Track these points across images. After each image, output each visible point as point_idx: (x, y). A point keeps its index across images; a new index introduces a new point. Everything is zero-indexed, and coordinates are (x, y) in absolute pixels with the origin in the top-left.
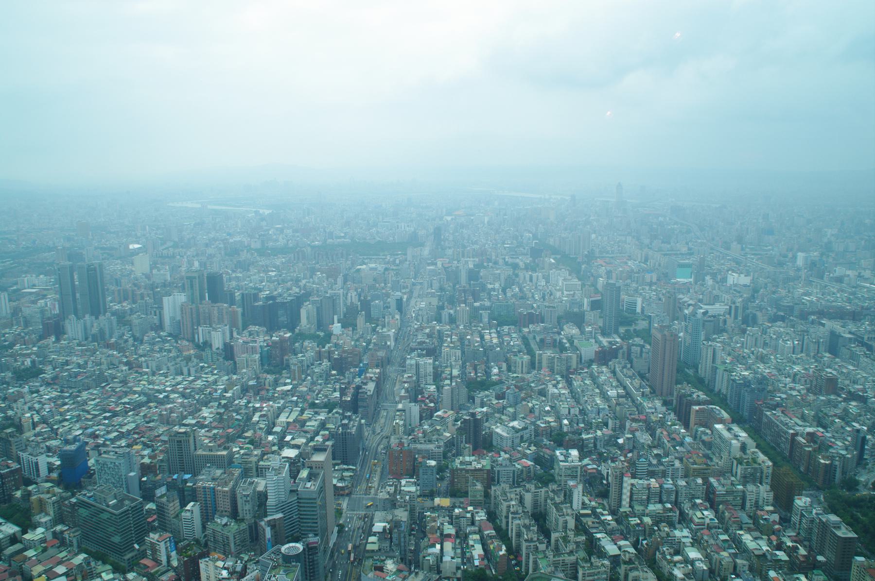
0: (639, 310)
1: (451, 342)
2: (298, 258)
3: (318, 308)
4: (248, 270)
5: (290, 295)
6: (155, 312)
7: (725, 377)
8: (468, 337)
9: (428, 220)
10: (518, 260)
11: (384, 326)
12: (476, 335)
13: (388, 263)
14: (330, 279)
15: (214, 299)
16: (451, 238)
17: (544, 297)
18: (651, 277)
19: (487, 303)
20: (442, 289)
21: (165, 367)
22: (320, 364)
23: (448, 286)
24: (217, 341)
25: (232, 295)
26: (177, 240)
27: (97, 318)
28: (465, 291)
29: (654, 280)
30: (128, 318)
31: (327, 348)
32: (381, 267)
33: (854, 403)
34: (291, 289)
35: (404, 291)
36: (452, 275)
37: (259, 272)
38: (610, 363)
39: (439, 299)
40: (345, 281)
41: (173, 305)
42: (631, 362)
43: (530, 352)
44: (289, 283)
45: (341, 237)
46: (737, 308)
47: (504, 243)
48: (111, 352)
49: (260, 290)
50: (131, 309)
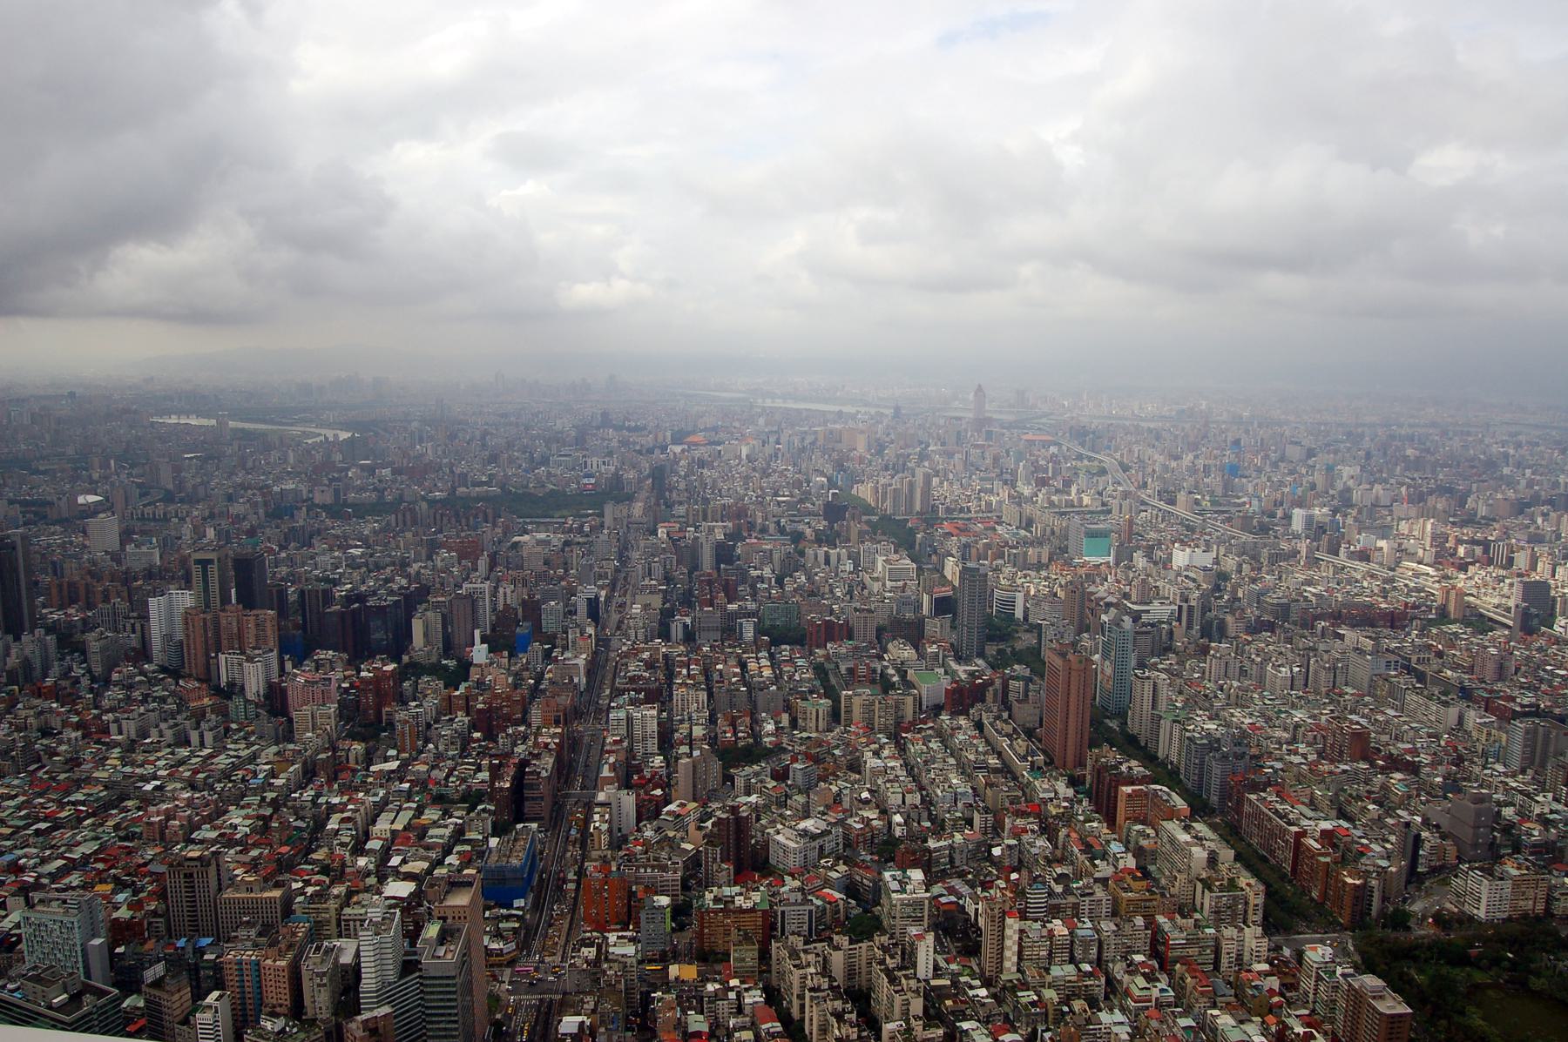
0: (1019, 614)
2: (405, 523)
3: (444, 617)
4: (310, 545)
5: (391, 592)
6: (133, 625)
8: (720, 667)
9: (640, 452)
11: (565, 648)
12: (732, 662)
13: (570, 530)
15: (248, 600)
16: (682, 486)
17: (850, 592)
19: (751, 606)
20: (668, 579)
21: (154, 731)
23: (680, 572)
24: (254, 680)
25: (282, 593)
26: (170, 487)
27: (17, 639)
28: (710, 583)
29: (1045, 560)
30: (78, 637)
32: (557, 539)
33: (1398, 776)
34: (391, 580)
35: (600, 583)
36: (688, 555)
37: (331, 550)
40: (492, 565)
41: (169, 609)
42: (1009, 709)
44: (389, 569)
45: (482, 484)
46: (1190, 608)
47: (776, 494)
48: (46, 704)
49: (335, 583)
50: (84, 621)
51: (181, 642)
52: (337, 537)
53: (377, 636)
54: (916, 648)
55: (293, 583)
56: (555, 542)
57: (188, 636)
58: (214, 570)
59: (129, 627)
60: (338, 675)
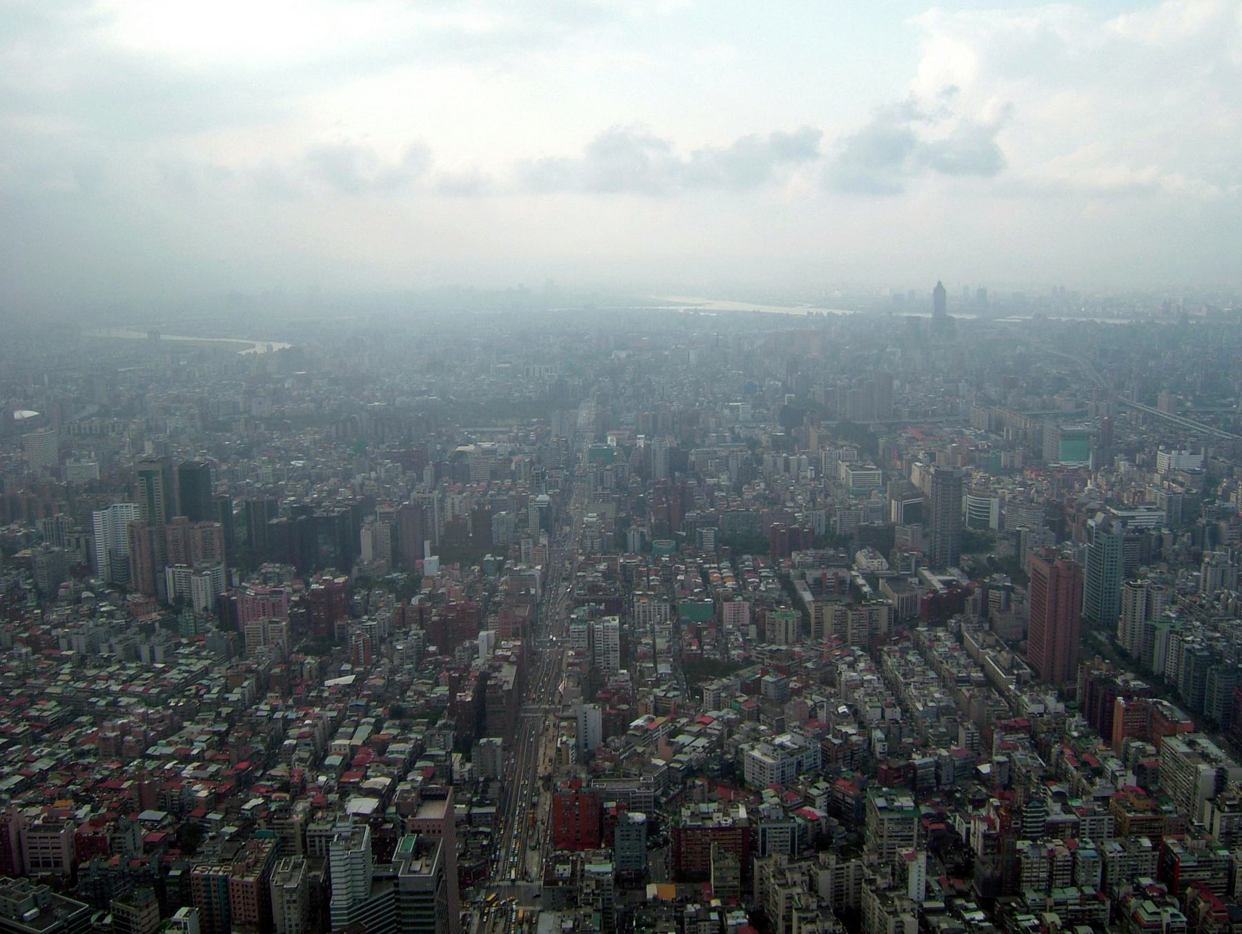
3: (394, 530)
6: (78, 540)
10: (757, 431)
11: (518, 560)
13: (516, 438)
14: (409, 473)
17: (813, 500)
22: (406, 633)
25: (227, 506)
29: (1018, 463)
31: (415, 601)
39: (619, 510)
40: (438, 476)
41: (114, 525)
42: (991, 621)
43: (798, 603)
44: (332, 481)
45: (422, 393)
51: (126, 560)
52: (277, 449)
53: (325, 548)
54: (886, 556)
55: (235, 496)
57: (133, 550)
58: (158, 482)
59: (73, 541)
60: (290, 589)
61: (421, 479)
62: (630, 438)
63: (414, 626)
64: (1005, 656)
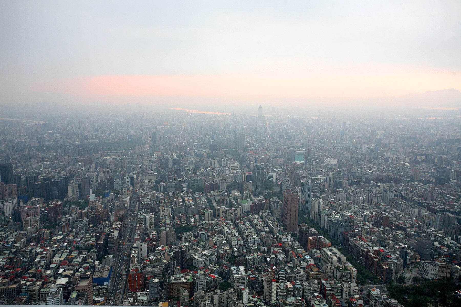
0: (274, 180)
1: (165, 203)
2: (65, 153)
3: (79, 185)
4: (30, 161)
5: (60, 177)
7: (326, 218)
8: (175, 200)
11: (122, 195)
12: (179, 198)
13: (124, 155)
14: (86, 166)
16: (162, 139)
17: (219, 174)
18: (281, 162)
19: (186, 179)
20: (157, 171)
23: (162, 169)
25: (19, 178)
28: (172, 172)
29: (282, 163)
32: (119, 158)
34: (61, 173)
35: (134, 172)
36: (164, 162)
37: (38, 163)
38: (260, 213)
39: (157, 177)
40: (96, 167)
42: (271, 211)
43: (212, 207)
49: (39, 174)
52: (40, 158)
55: (23, 174)
56: (118, 158)
61: (91, 169)
62: (162, 154)
63: (85, 218)
64: (276, 223)
